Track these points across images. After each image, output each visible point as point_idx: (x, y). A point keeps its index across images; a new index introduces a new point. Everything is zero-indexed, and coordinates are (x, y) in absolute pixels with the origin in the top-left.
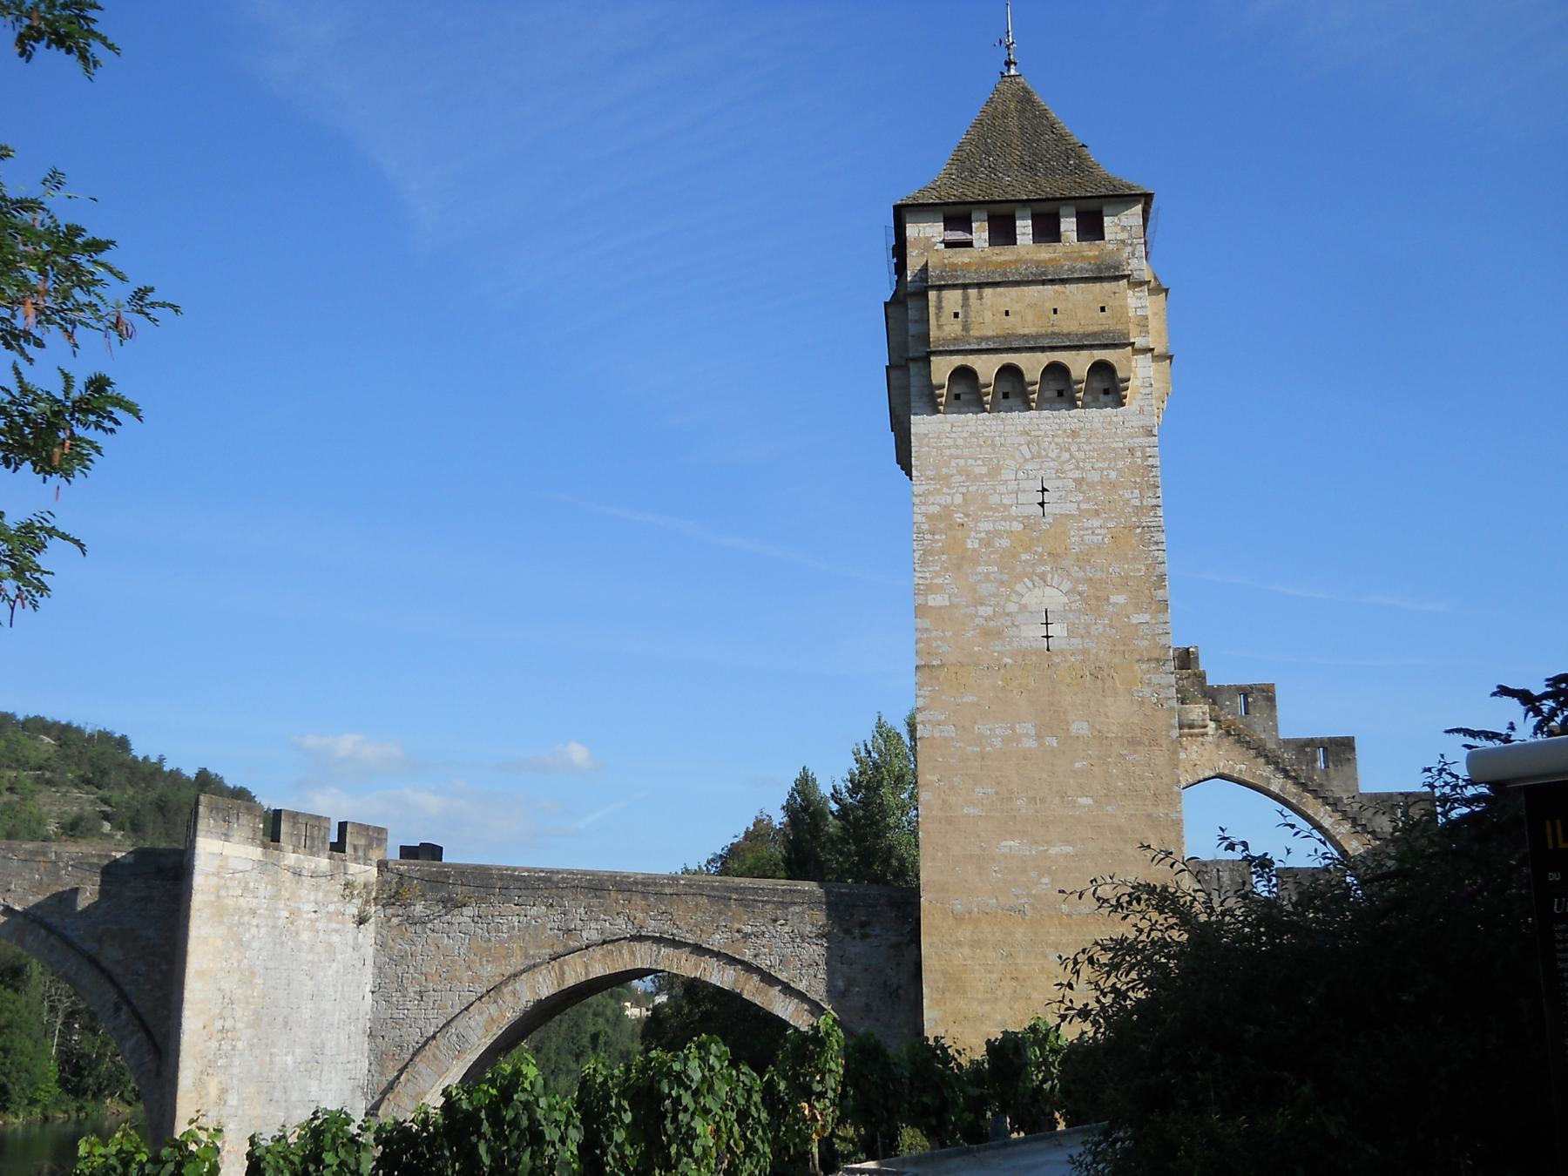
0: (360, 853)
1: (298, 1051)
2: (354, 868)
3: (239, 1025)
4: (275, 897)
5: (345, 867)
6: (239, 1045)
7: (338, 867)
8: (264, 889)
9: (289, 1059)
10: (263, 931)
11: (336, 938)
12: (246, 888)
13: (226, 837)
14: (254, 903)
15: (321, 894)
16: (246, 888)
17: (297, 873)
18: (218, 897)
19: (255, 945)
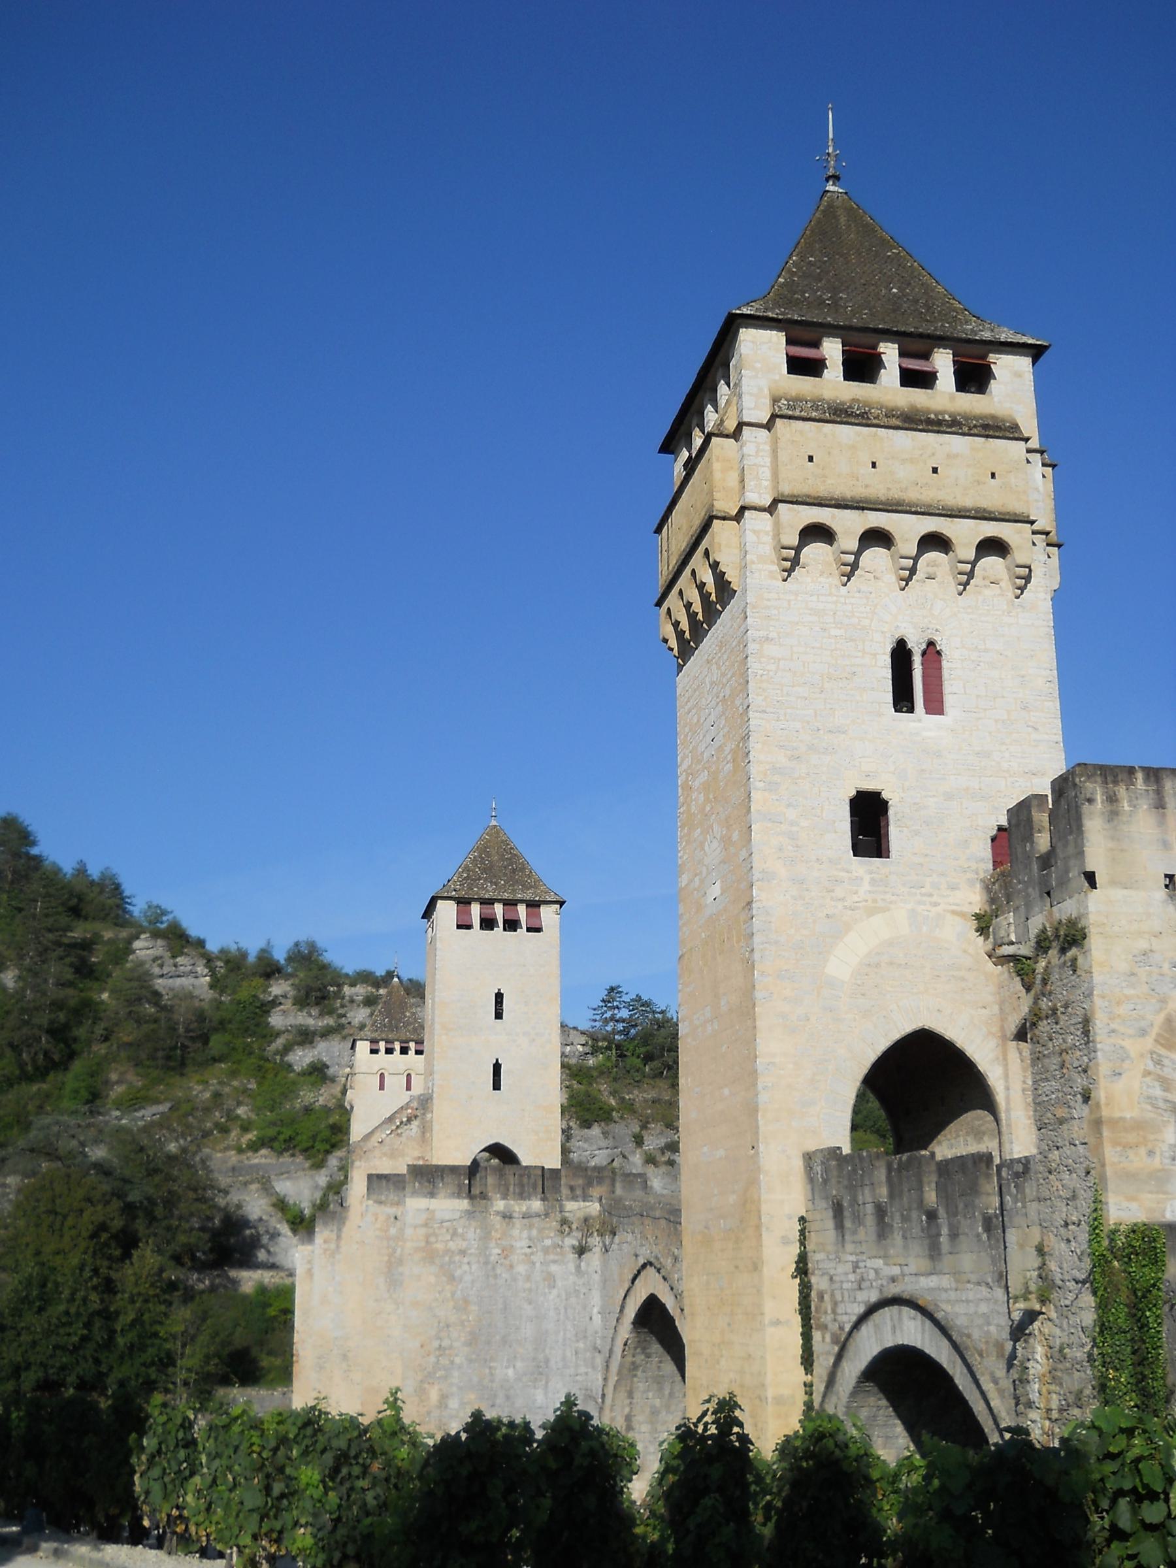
0: (579, 1192)
1: (519, 1364)
2: (570, 1206)
3: (456, 1344)
4: (486, 1237)
5: (561, 1206)
6: (457, 1360)
7: (553, 1207)
8: (472, 1233)
9: (510, 1372)
10: (474, 1267)
11: (554, 1268)
12: (454, 1234)
13: (432, 1195)
14: (464, 1245)
15: (534, 1232)
16: (454, 1234)
17: (507, 1216)
18: (427, 1242)
19: (468, 1278)
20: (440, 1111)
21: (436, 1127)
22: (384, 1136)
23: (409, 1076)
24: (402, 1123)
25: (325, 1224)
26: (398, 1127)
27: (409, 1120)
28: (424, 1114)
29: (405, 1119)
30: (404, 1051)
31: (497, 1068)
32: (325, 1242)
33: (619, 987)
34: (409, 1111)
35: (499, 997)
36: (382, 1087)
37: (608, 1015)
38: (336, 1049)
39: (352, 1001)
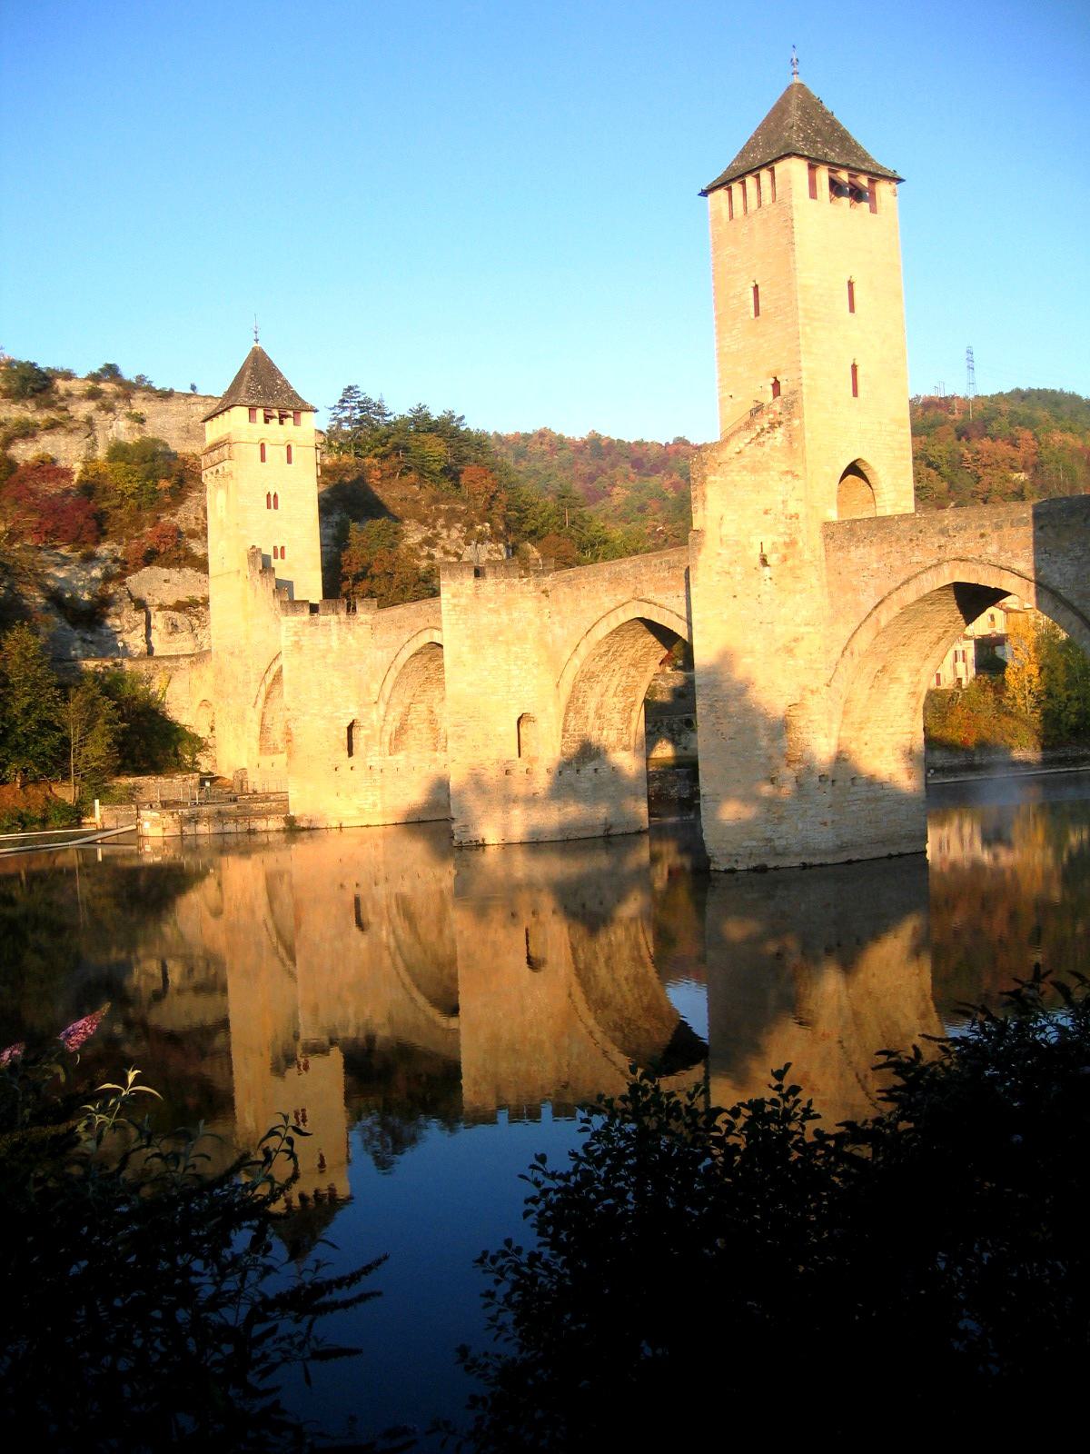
20: (813, 417)
21: (808, 435)
22: (742, 445)
23: (289, 448)
24: (762, 430)
25: (453, 576)
26: (758, 435)
27: (772, 426)
28: (789, 420)
29: (766, 426)
30: (282, 418)
31: (854, 368)
32: (454, 596)
33: (357, 387)
34: (771, 416)
35: (850, 284)
36: (263, 459)
37: (347, 414)
38: (62, 443)
39: (70, 395)
